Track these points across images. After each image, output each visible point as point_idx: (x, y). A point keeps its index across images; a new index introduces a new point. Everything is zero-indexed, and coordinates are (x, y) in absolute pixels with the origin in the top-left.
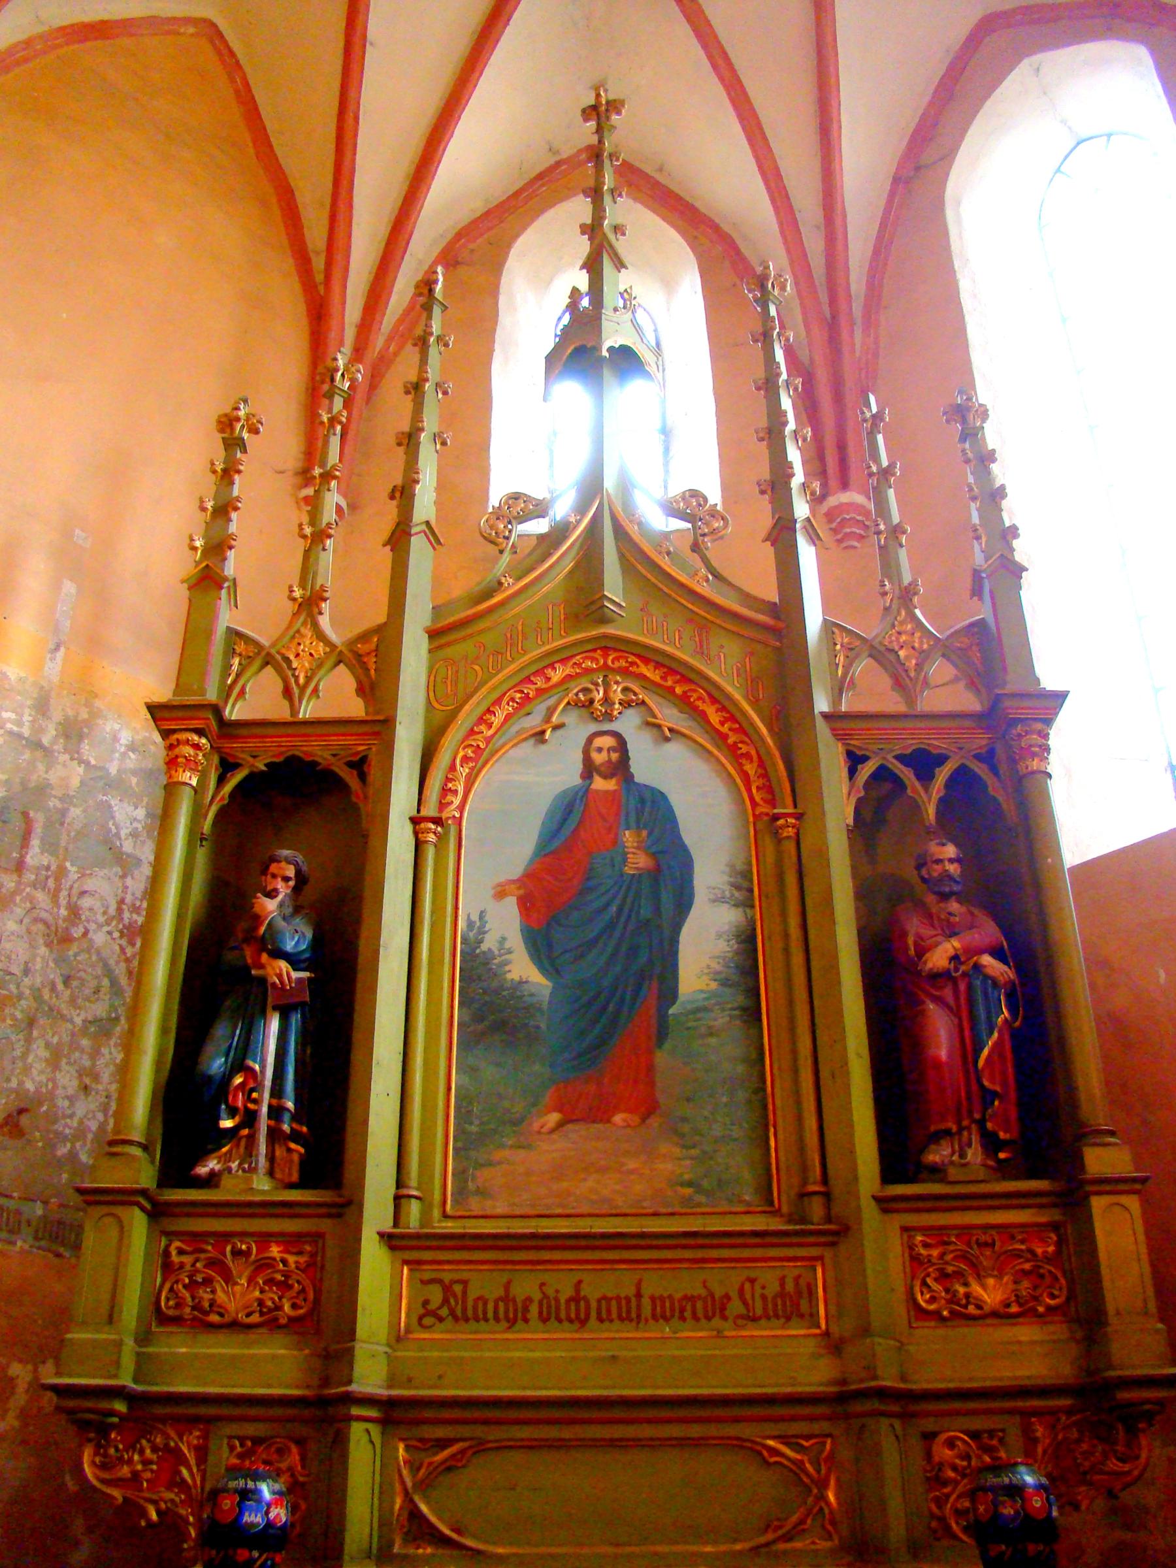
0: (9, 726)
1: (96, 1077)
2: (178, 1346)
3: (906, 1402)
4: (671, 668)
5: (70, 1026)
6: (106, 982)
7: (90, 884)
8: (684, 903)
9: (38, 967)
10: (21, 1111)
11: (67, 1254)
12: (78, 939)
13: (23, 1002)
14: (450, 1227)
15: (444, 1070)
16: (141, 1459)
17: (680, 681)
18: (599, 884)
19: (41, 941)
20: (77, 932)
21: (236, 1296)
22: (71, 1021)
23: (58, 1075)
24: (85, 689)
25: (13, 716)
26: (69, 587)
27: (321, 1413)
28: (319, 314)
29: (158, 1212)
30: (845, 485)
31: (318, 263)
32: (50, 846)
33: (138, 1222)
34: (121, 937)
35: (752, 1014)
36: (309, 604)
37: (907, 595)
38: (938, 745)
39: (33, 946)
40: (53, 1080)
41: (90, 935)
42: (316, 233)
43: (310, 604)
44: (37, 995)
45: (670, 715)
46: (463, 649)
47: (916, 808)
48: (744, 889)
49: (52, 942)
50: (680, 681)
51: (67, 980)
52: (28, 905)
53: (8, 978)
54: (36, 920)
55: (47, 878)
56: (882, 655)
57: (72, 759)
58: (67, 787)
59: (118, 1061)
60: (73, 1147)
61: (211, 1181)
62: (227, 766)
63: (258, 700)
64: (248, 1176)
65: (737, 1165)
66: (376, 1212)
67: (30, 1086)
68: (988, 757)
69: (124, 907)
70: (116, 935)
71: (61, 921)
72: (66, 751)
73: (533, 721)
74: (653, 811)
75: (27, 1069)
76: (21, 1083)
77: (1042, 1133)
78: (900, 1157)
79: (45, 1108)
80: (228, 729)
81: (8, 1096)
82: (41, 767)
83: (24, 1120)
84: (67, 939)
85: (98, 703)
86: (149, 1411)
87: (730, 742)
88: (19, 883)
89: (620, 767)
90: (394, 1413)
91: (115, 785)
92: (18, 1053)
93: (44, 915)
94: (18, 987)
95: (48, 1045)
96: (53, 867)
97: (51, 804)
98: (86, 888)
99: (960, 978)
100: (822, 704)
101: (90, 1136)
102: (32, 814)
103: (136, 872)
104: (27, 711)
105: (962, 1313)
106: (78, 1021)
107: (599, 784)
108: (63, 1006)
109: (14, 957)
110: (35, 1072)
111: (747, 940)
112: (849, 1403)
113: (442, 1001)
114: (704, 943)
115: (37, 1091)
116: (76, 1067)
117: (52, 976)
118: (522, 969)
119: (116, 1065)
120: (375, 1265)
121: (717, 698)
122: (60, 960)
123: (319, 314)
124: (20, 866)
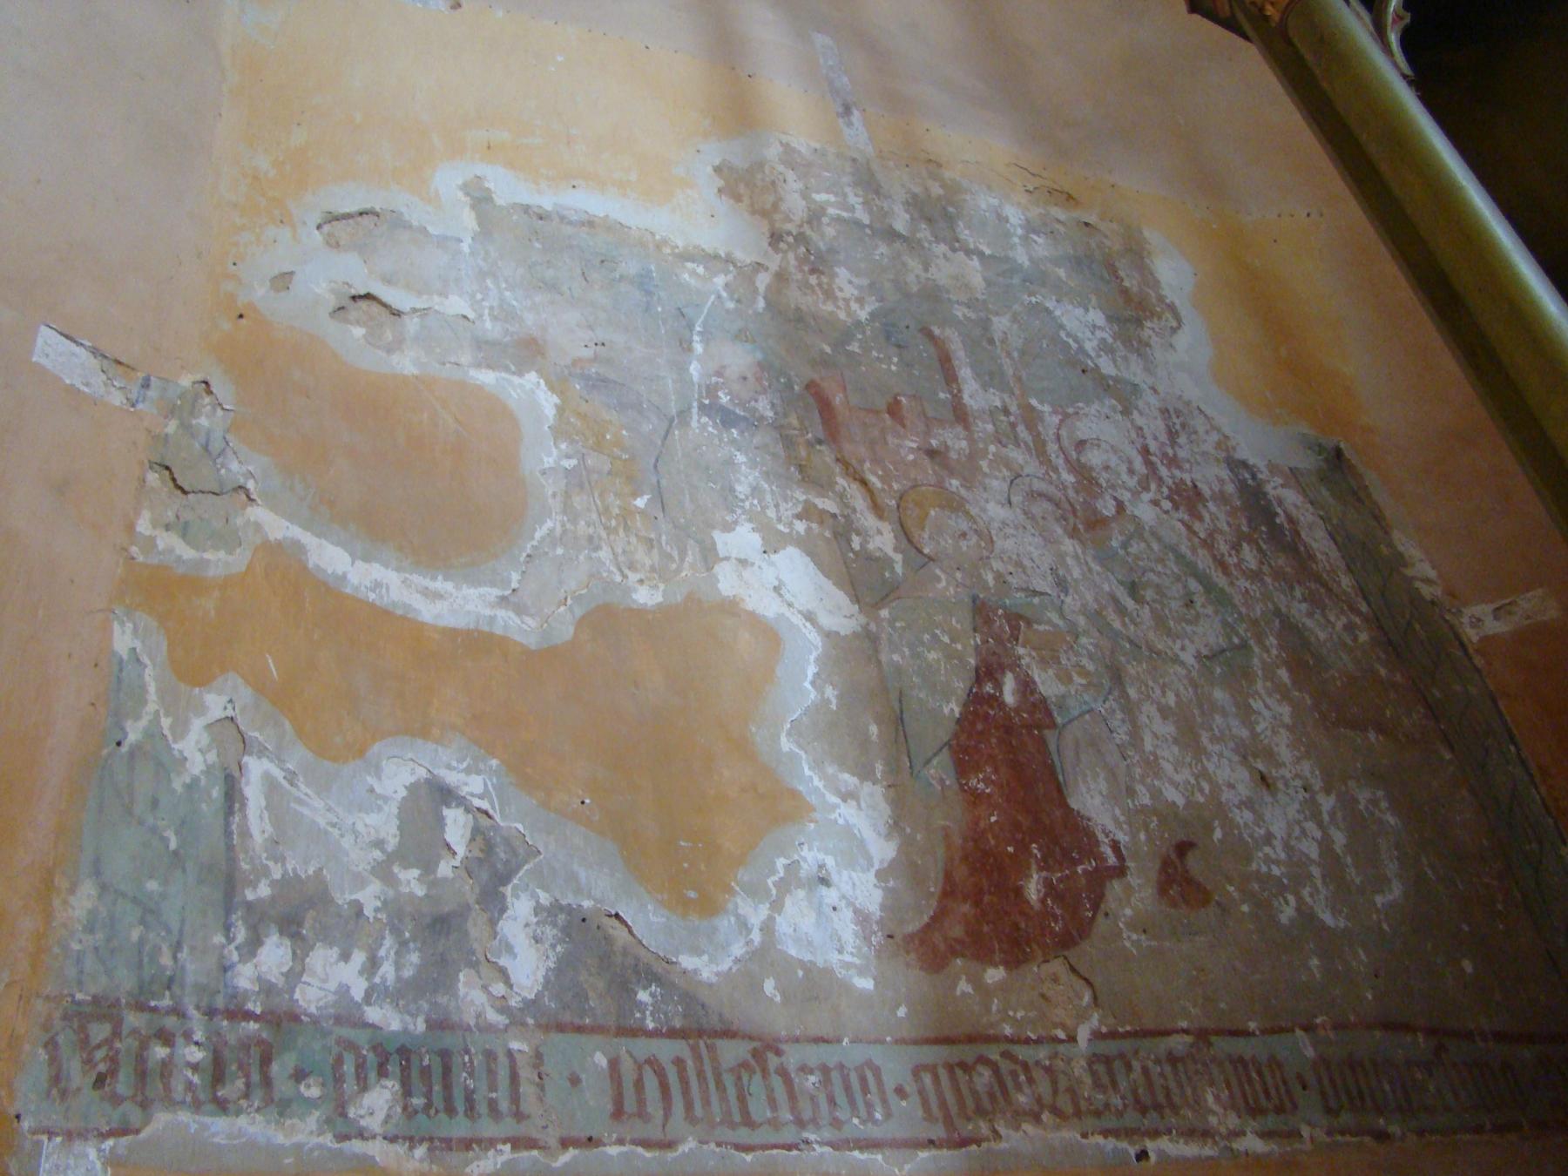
0: (831, 211)
1: (1270, 755)
5: (1179, 669)
6: (1193, 585)
7: (1084, 429)
9: (1076, 573)
10: (1183, 848)
11: (1394, 1129)
12: (1114, 518)
13: (1084, 640)
19: (1060, 531)
20: (1107, 508)
22: (1176, 660)
23: (1211, 767)
25: (832, 198)
26: (821, 40)
32: (991, 377)
34: (1176, 507)
39: (1049, 540)
40: (1204, 774)
41: (1129, 509)
44: (1096, 617)
49: (1075, 529)
51: (1133, 589)
52: (1006, 473)
53: (1036, 600)
54: (1034, 495)
55: (1013, 426)
57: (954, 250)
58: (967, 286)
59: (1287, 720)
60: (1299, 899)
67: (1173, 795)
69: (1153, 459)
70: (1167, 505)
71: (1071, 493)
72: (938, 240)
75: (1152, 765)
76: (1156, 794)
79: (1218, 834)
81: (1146, 827)
82: (914, 264)
83: (1195, 864)
84: (1096, 523)
85: (947, 174)
88: (971, 441)
91: (1037, 278)
92: (1122, 735)
93: (1038, 485)
94: (1062, 616)
95: (1164, 712)
96: (1013, 409)
97: (959, 314)
98: (1081, 435)
101: (1316, 871)
102: (937, 331)
103: (1140, 404)
104: (848, 190)
106: (1188, 658)
108: (1151, 635)
109: (1027, 563)
110: (1168, 768)
115: (1189, 804)
116: (1232, 745)
117: (1106, 587)
119: (1287, 727)
122: (1106, 559)
124: (961, 415)
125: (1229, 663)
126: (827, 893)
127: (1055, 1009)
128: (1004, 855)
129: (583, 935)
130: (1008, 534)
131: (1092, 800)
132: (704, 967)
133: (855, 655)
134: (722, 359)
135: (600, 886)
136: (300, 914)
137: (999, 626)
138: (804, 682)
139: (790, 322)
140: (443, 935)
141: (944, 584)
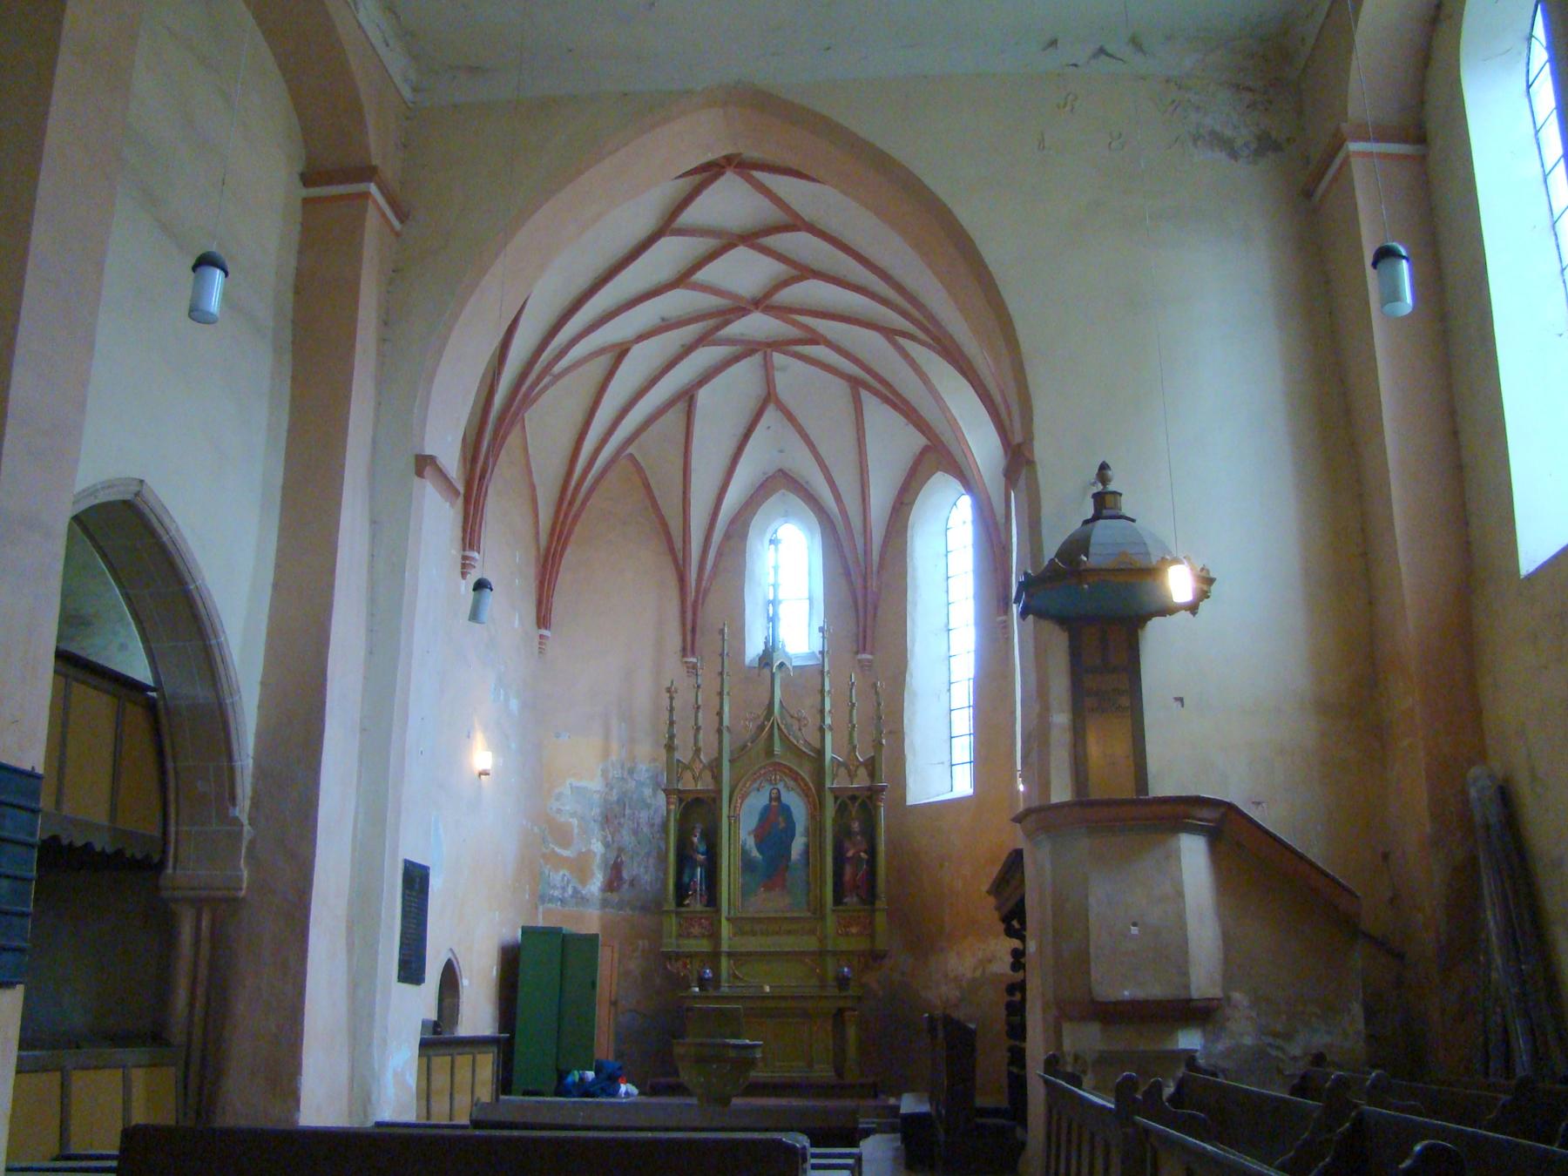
3: (834, 953)
4: (791, 770)
8: (793, 835)
16: (680, 963)
17: (796, 777)
21: (696, 930)
27: (714, 957)
28: (682, 580)
29: (677, 914)
30: (864, 650)
31: (680, 556)
33: (674, 920)
36: (697, 751)
42: (678, 545)
43: (697, 751)
45: (791, 783)
48: (807, 833)
50: (796, 777)
62: (681, 800)
64: (696, 904)
66: (724, 913)
68: (870, 798)
73: (756, 785)
74: (786, 811)
78: (838, 900)
87: (806, 793)
89: (778, 798)
90: (730, 955)
91: (643, 784)
99: (856, 860)
100: (828, 784)
111: (807, 846)
112: (821, 954)
113: (738, 862)
114: (798, 845)
118: (755, 853)
123: (682, 580)
125: (648, 855)
126: (595, 885)
127: (615, 897)
128: (614, 880)
129: (575, 889)
130: (627, 838)
131: (625, 875)
134: (596, 811)
136: (554, 887)
137: (621, 850)
138: (598, 860)
140: (564, 889)
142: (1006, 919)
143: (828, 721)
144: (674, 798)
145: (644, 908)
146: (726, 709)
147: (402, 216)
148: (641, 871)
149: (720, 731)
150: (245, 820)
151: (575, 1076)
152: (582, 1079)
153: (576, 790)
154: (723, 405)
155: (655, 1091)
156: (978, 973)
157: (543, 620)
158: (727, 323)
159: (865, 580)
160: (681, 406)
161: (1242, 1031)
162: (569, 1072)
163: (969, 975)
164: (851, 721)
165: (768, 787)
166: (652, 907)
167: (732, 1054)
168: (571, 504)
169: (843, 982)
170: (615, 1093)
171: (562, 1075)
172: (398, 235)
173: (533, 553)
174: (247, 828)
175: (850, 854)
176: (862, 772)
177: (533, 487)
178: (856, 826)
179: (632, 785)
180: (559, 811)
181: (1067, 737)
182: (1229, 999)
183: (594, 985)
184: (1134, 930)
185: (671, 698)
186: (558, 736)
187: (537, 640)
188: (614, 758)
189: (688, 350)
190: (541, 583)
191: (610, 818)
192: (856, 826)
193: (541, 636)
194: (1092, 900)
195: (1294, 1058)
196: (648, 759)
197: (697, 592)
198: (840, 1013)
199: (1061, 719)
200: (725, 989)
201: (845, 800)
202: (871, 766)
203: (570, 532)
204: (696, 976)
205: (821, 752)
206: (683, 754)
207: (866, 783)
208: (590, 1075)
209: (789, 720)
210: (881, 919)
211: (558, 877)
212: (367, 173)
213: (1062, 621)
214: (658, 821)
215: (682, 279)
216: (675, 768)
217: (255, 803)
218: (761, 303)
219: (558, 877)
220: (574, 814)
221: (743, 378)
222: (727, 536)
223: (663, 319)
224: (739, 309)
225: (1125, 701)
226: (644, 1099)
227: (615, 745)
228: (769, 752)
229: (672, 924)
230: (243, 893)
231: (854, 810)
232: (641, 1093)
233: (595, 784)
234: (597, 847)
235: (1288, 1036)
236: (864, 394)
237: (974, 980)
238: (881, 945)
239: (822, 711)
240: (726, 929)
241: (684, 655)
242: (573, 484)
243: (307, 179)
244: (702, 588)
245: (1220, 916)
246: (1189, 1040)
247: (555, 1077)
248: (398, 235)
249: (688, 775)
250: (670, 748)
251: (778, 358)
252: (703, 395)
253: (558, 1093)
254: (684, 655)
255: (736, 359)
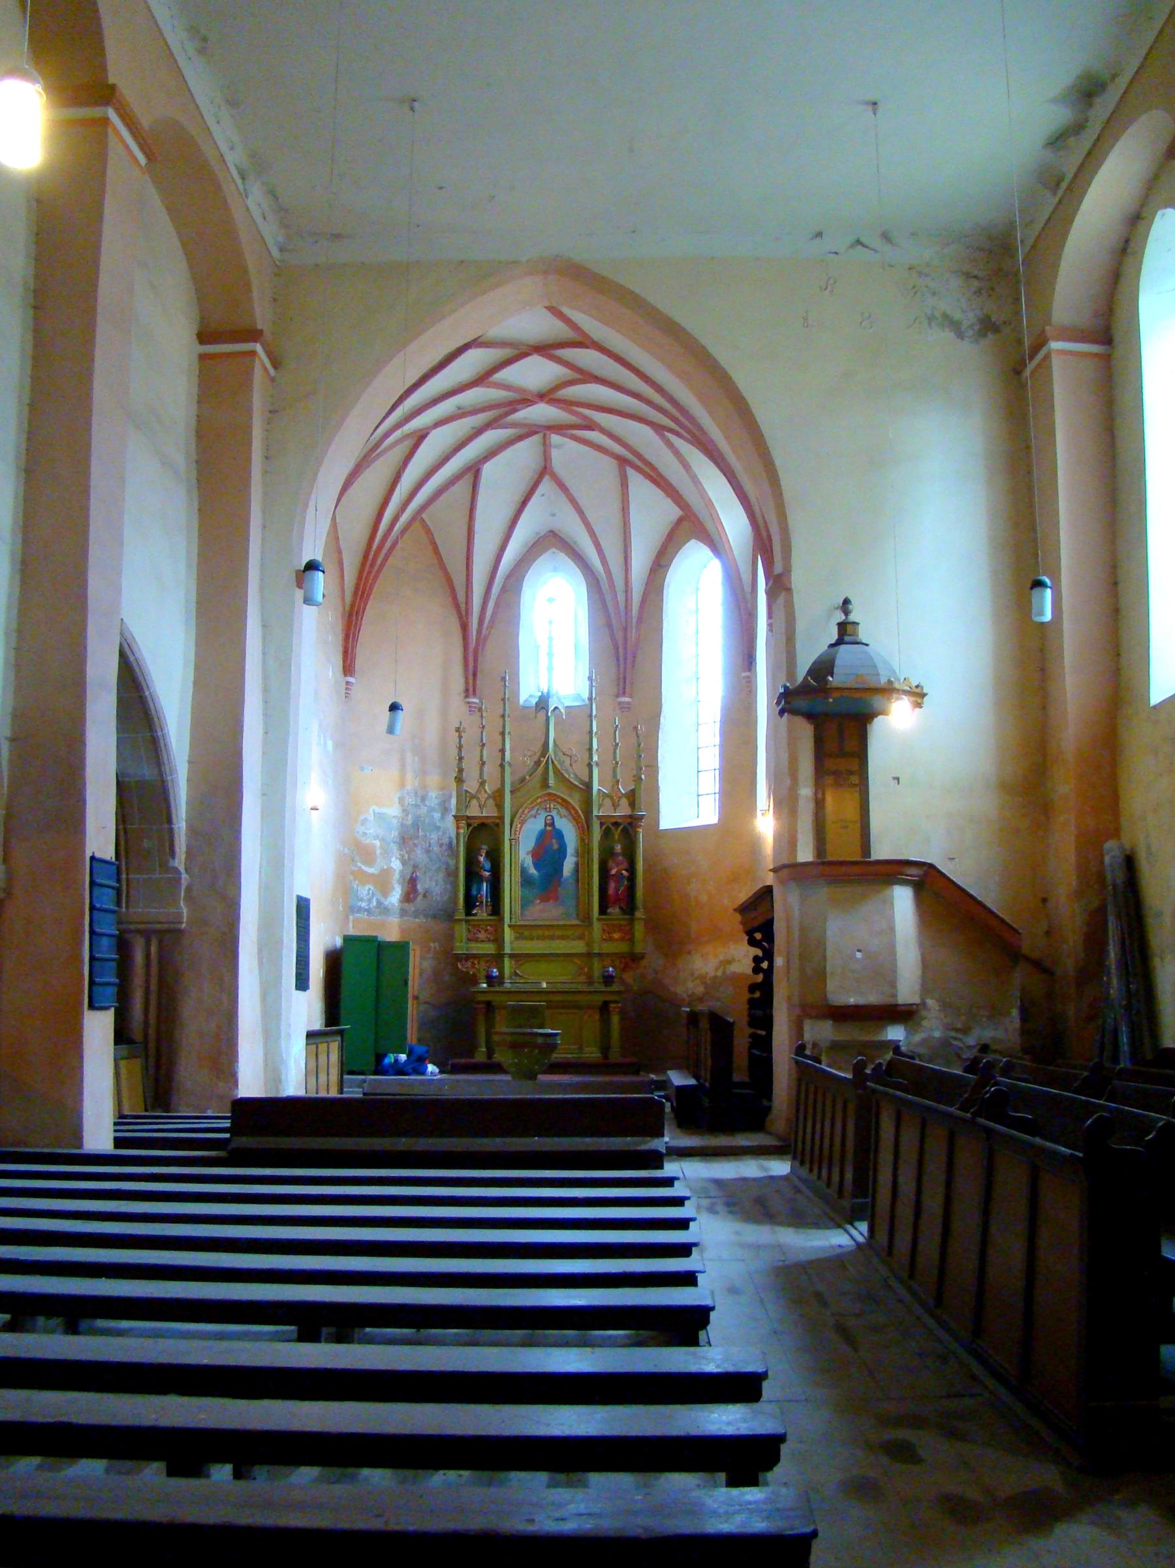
2: (473, 945)
3: (600, 955)
4: (564, 800)
14: (522, 923)
15: (518, 892)
16: (469, 964)
17: (565, 804)
18: (548, 850)
21: (482, 936)
24: (424, 786)
27: (498, 958)
28: (465, 627)
29: (467, 921)
30: (624, 694)
31: (463, 606)
33: (464, 925)
35: (577, 881)
36: (483, 784)
37: (618, 782)
38: (620, 821)
43: (482, 783)
45: (563, 811)
46: (518, 794)
47: (613, 835)
48: (577, 854)
50: (565, 804)
56: (612, 798)
61: (475, 915)
62: (469, 825)
63: (474, 811)
65: (572, 911)
68: (630, 824)
73: (534, 812)
74: (559, 835)
77: (629, 906)
78: (603, 910)
80: (468, 818)
86: (468, 957)
87: (576, 819)
89: (552, 824)
90: (512, 956)
100: (595, 813)
105: (611, 939)
107: (549, 828)
111: (577, 864)
112: (589, 955)
113: (517, 878)
118: (533, 871)
120: (507, 930)
121: (574, 808)
123: (465, 627)
126: (395, 897)
127: (411, 907)
128: (410, 893)
129: (378, 902)
130: (420, 855)
131: (419, 887)
132: (386, 903)
133: (401, 872)
134: (395, 834)
135: (380, 897)
137: (415, 867)
138: (397, 876)
139: (403, 825)
140: (370, 901)
141: (412, 863)
142: (750, 933)
143: (595, 758)
144: (463, 823)
145: (434, 917)
146: (508, 747)
147: (276, 366)
148: (434, 884)
149: (502, 766)
150: (182, 868)
151: (390, 1058)
152: (396, 1060)
153: (380, 817)
154: (503, 476)
155: (456, 1069)
156: (719, 973)
157: (348, 668)
158: (515, 411)
159: (625, 629)
160: (469, 478)
161: (933, 1027)
162: (385, 1055)
163: (712, 973)
164: (615, 757)
165: (543, 814)
166: (447, 915)
167: (540, 1040)
168: (372, 566)
169: (608, 979)
170: (423, 1073)
171: (380, 1057)
172: (273, 380)
173: (341, 609)
174: (184, 876)
175: (613, 872)
176: (624, 802)
177: (340, 552)
178: (618, 848)
179: (424, 810)
180: (365, 834)
181: (811, 806)
182: (924, 1004)
183: (406, 983)
184: (859, 955)
185: (460, 737)
186: (362, 769)
187: (344, 686)
188: (409, 787)
189: (479, 432)
190: (346, 638)
191: (406, 839)
192: (618, 848)
193: (348, 683)
194: (829, 933)
195: (970, 1047)
196: (436, 787)
197: (478, 639)
198: (606, 1004)
199: (806, 791)
200: (507, 985)
201: (609, 827)
202: (632, 797)
203: (371, 588)
204: (483, 973)
205: (589, 786)
206: (471, 785)
207: (628, 812)
208: (403, 1057)
209: (563, 758)
210: (639, 929)
211: (365, 890)
212: (254, 335)
213: (810, 716)
214: (446, 841)
215: (481, 379)
216: (465, 798)
217: (190, 853)
218: (545, 396)
219: (365, 890)
220: (376, 837)
221: (525, 454)
222: (504, 589)
223: (459, 408)
224: (526, 399)
225: (854, 779)
226: (444, 1076)
227: (409, 776)
228: (545, 783)
229: (461, 930)
230: (184, 925)
231: (617, 833)
232: (441, 1072)
233: (393, 811)
234: (396, 865)
235: (965, 1031)
236: (630, 472)
237: (715, 977)
238: (639, 949)
239: (590, 749)
240: (508, 934)
241: (467, 697)
242: (375, 547)
243: (204, 337)
244: (480, 639)
245: (921, 946)
246: (895, 1033)
247: (373, 1059)
248: (273, 380)
249: (474, 802)
250: (459, 780)
251: (555, 439)
252: (487, 469)
253: (376, 1073)
254: (467, 697)
255: (520, 438)
